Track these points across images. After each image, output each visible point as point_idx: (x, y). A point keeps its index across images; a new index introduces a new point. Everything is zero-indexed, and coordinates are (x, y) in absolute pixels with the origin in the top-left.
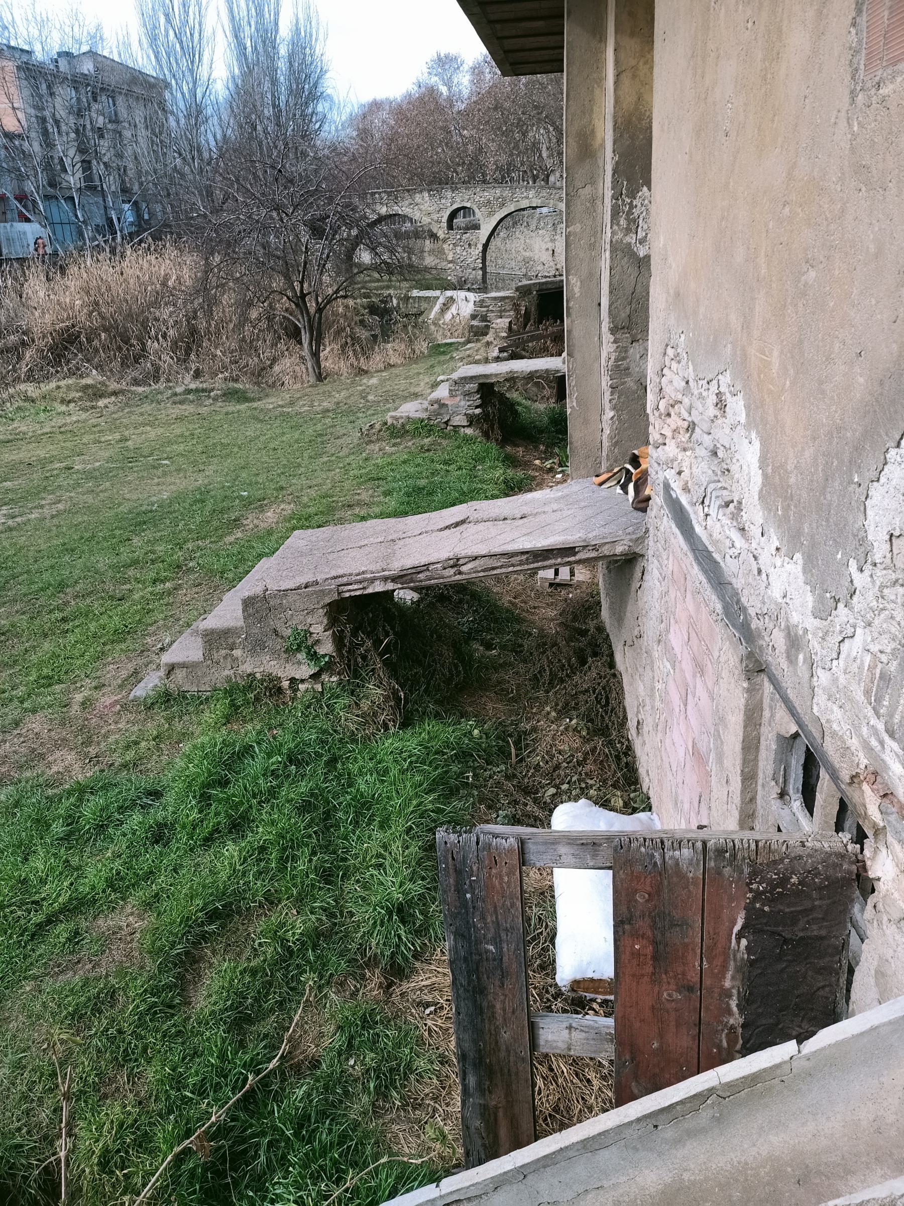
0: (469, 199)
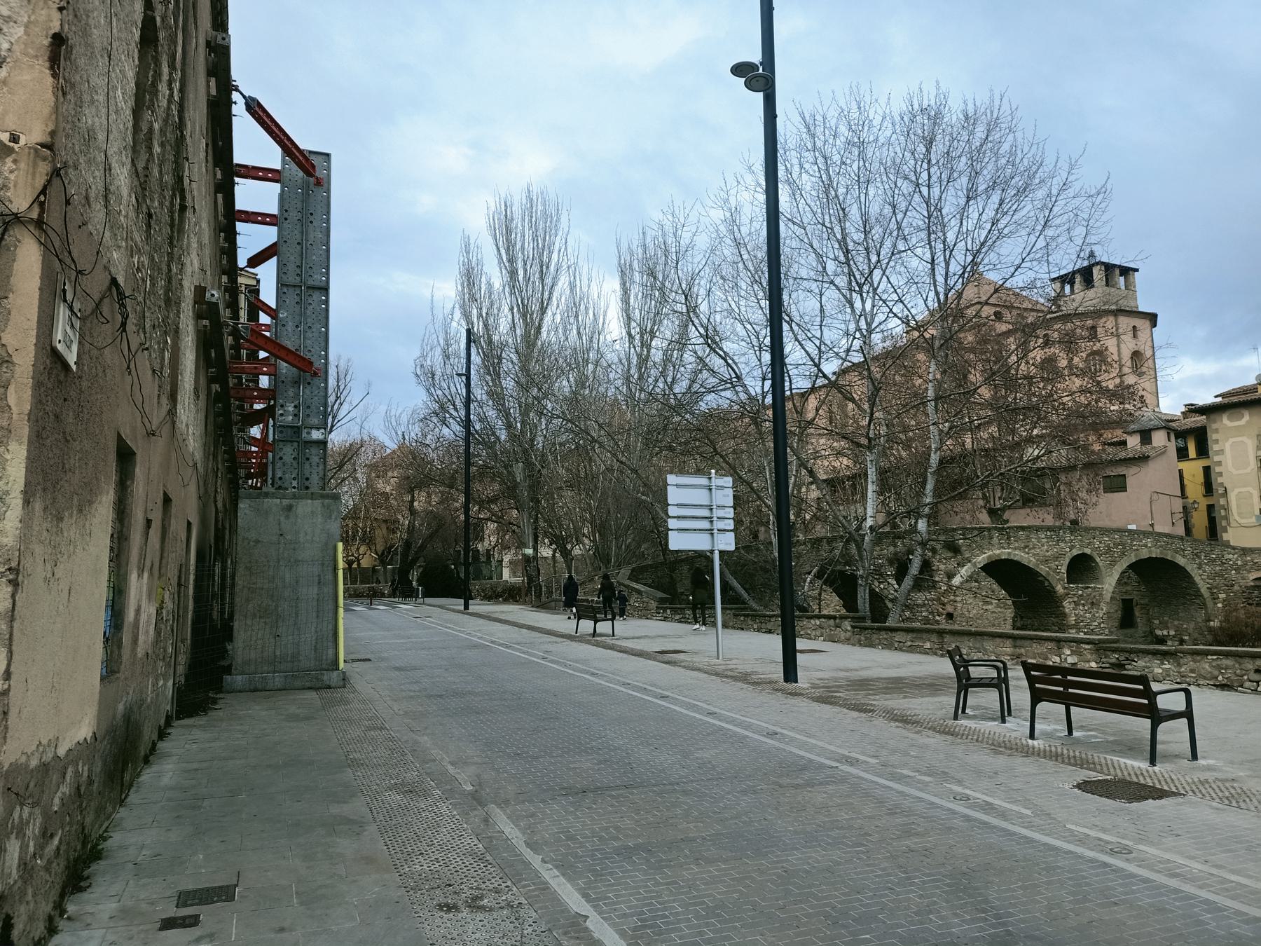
0: (1089, 544)
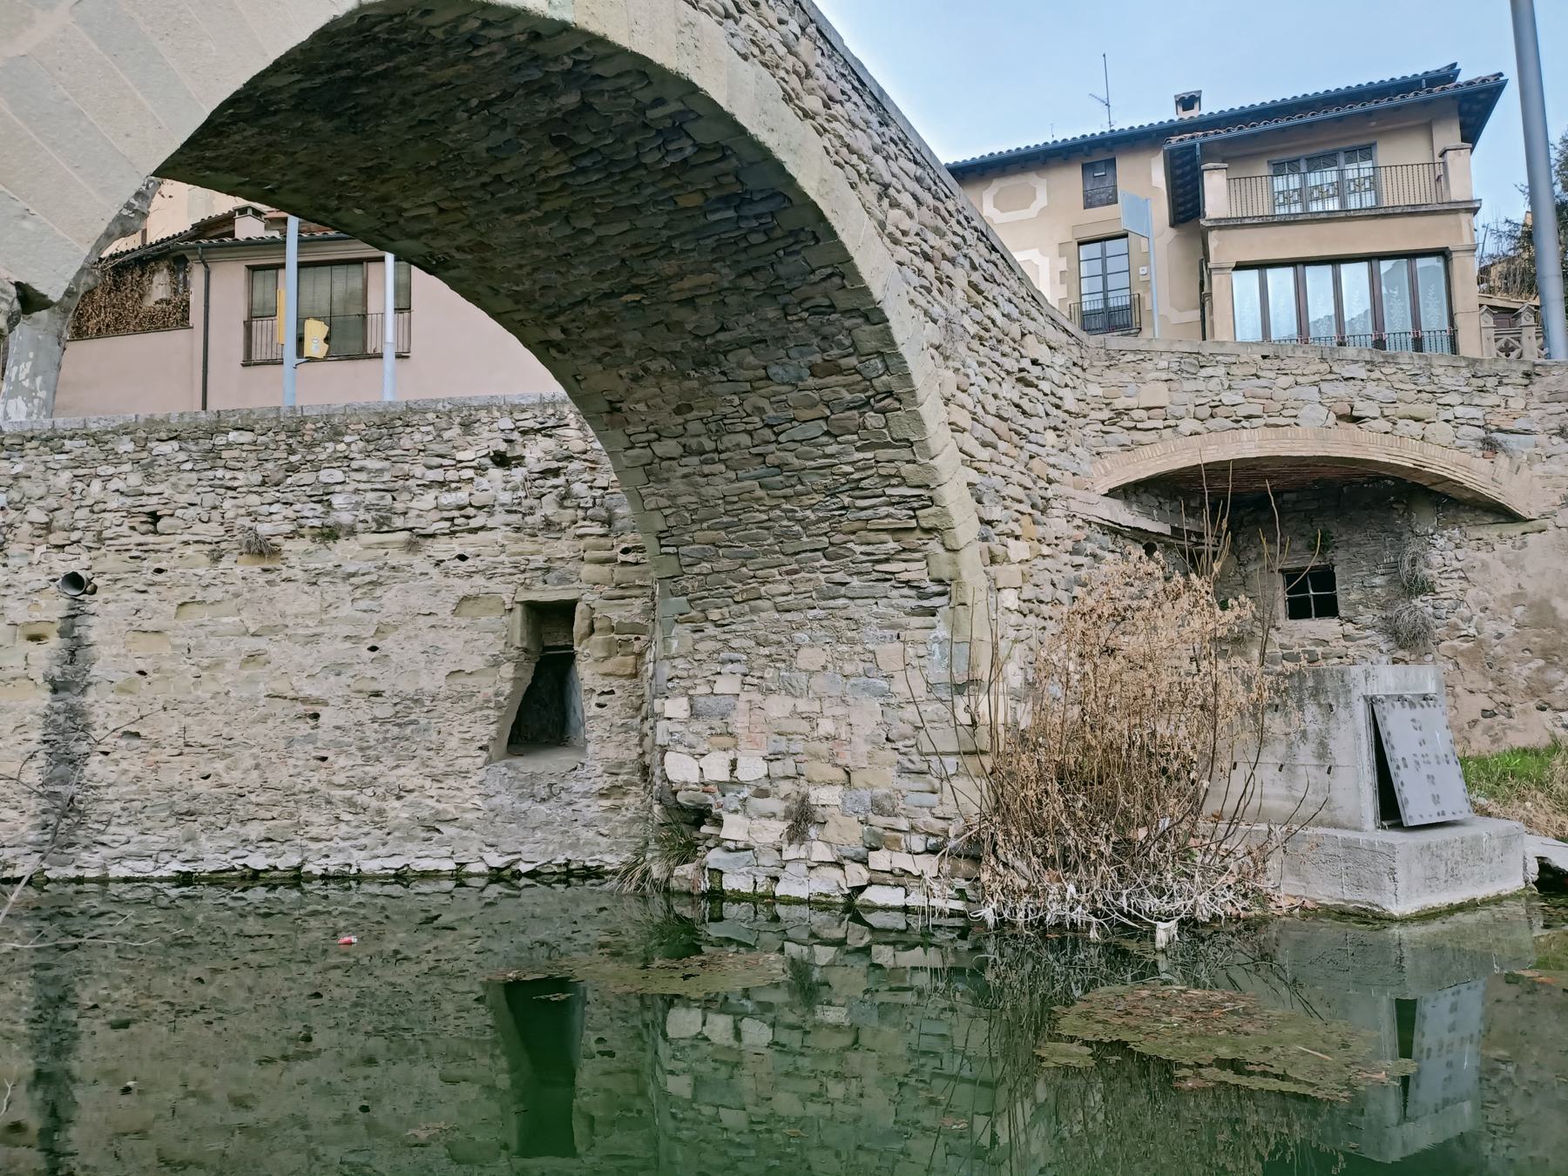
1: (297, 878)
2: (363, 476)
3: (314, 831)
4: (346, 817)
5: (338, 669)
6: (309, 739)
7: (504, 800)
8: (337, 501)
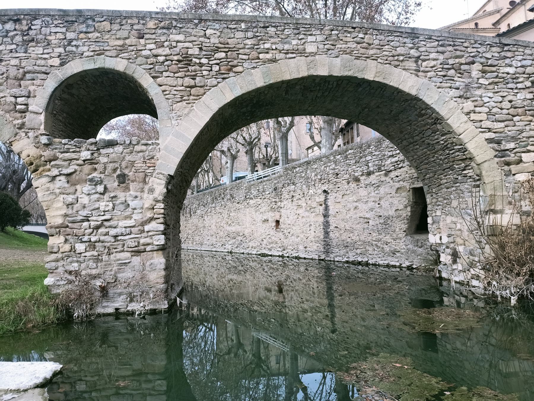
0: (123, 49)
1: (367, 264)
2: (375, 157)
3: (370, 252)
4: (376, 249)
5: (372, 210)
6: (368, 228)
7: (410, 246)
8: (370, 165)
